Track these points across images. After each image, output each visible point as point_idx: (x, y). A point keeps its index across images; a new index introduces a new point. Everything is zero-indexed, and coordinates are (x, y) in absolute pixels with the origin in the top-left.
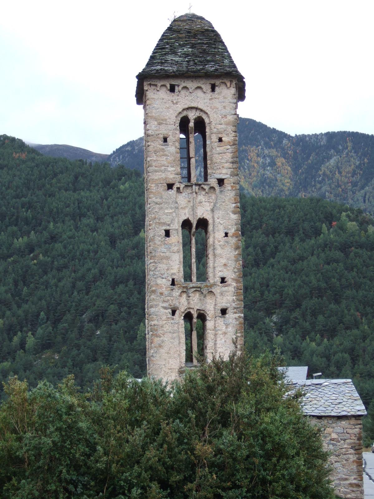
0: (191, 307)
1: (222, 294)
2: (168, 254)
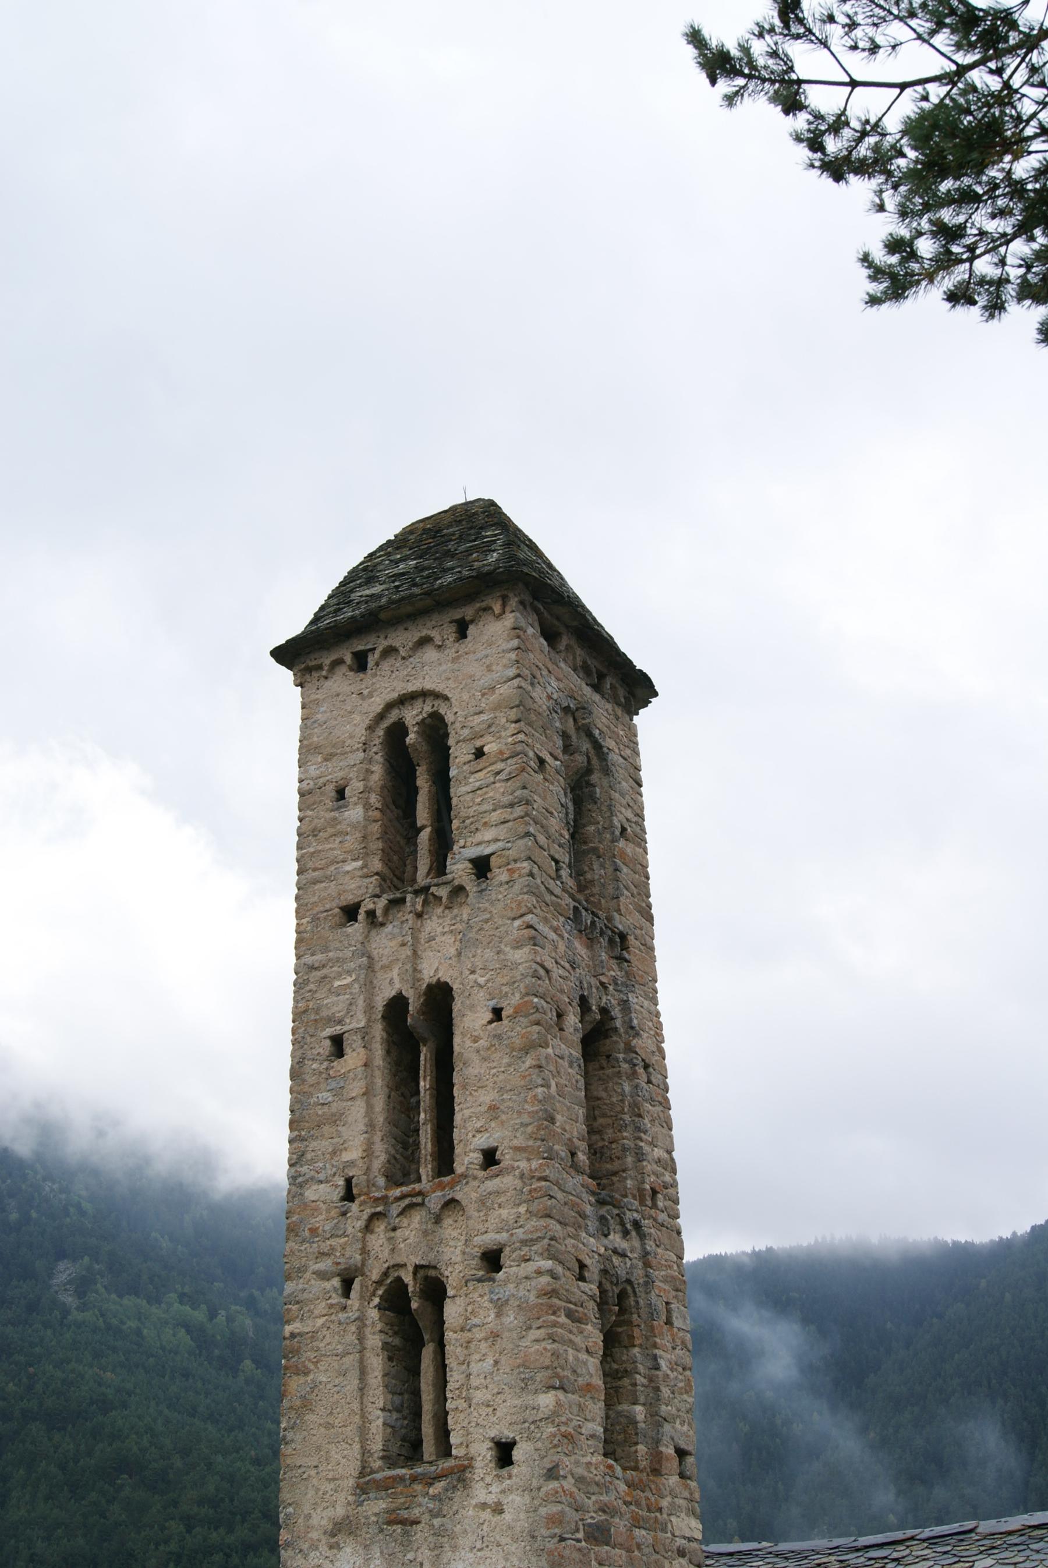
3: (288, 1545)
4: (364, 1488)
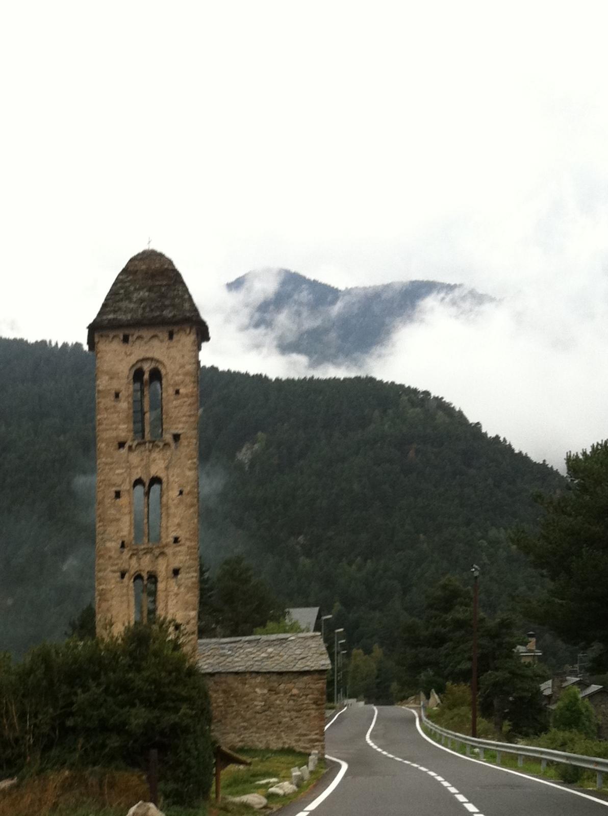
1: (174, 554)
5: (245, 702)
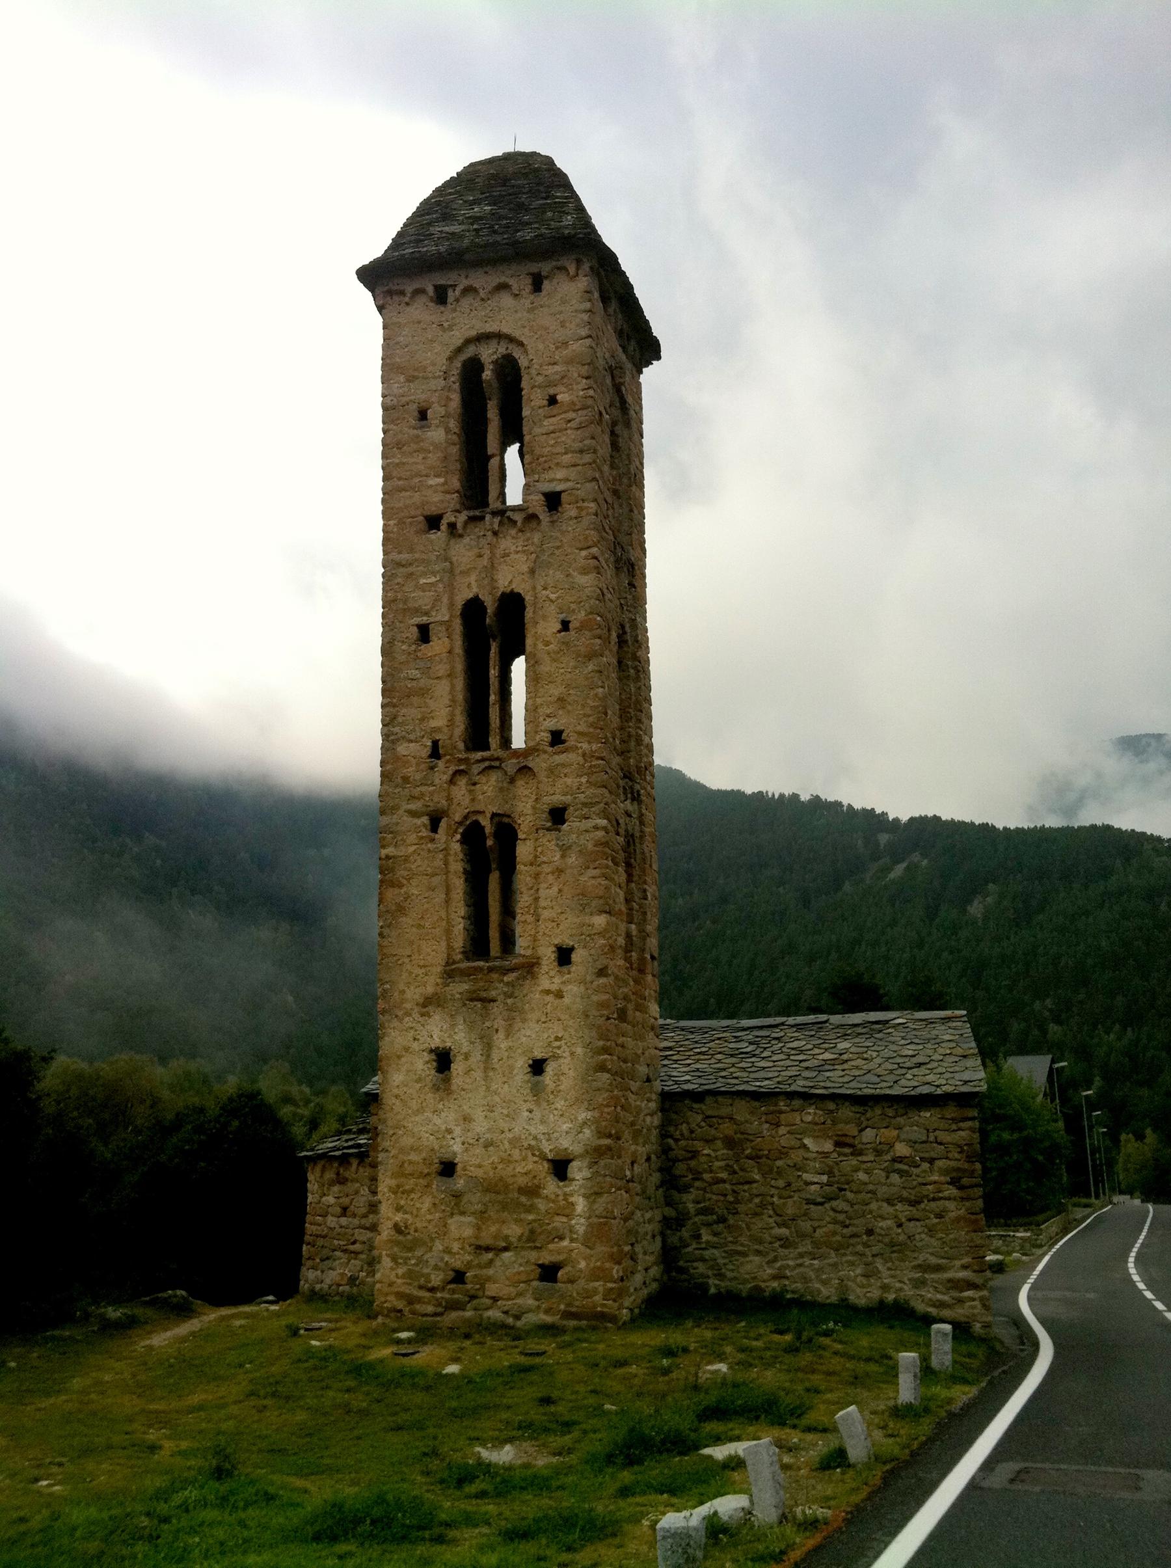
0: (478, 808)
1: (551, 771)
2: (423, 682)
3: (384, 1012)
4: (450, 973)
5: (780, 1173)
